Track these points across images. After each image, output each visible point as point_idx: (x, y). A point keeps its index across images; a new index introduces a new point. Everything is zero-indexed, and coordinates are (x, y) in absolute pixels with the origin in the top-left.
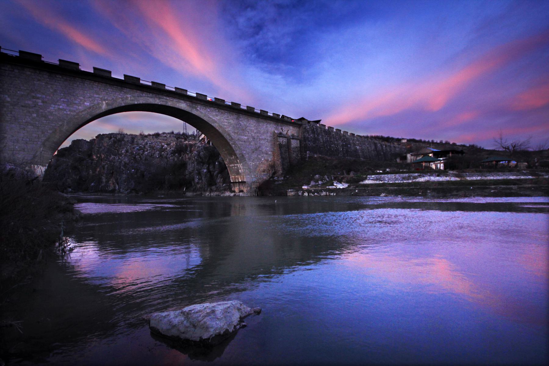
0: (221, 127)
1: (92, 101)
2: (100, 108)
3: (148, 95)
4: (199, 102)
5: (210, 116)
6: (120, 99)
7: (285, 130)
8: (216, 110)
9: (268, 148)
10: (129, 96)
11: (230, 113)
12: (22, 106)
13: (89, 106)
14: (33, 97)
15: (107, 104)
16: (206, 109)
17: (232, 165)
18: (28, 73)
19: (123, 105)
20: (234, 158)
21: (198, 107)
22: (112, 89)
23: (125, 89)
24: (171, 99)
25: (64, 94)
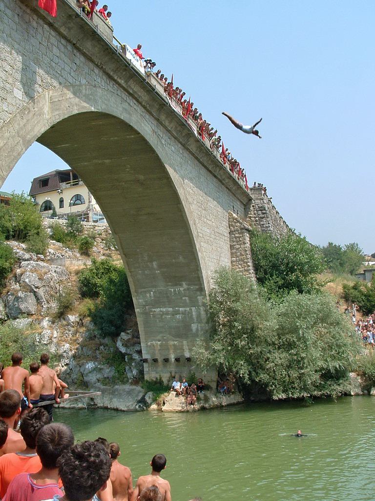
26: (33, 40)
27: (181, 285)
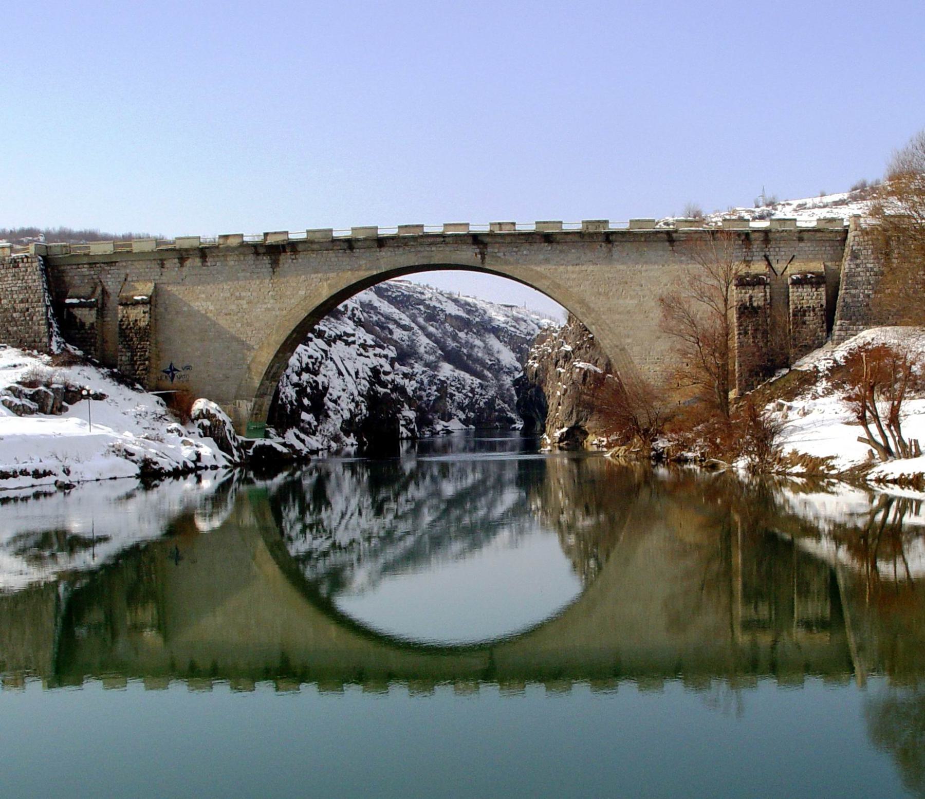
0: (559, 286)
2: (320, 294)
7: (777, 258)
10: (363, 262)
15: (330, 286)
16: (519, 251)
19: (354, 281)
21: (499, 252)
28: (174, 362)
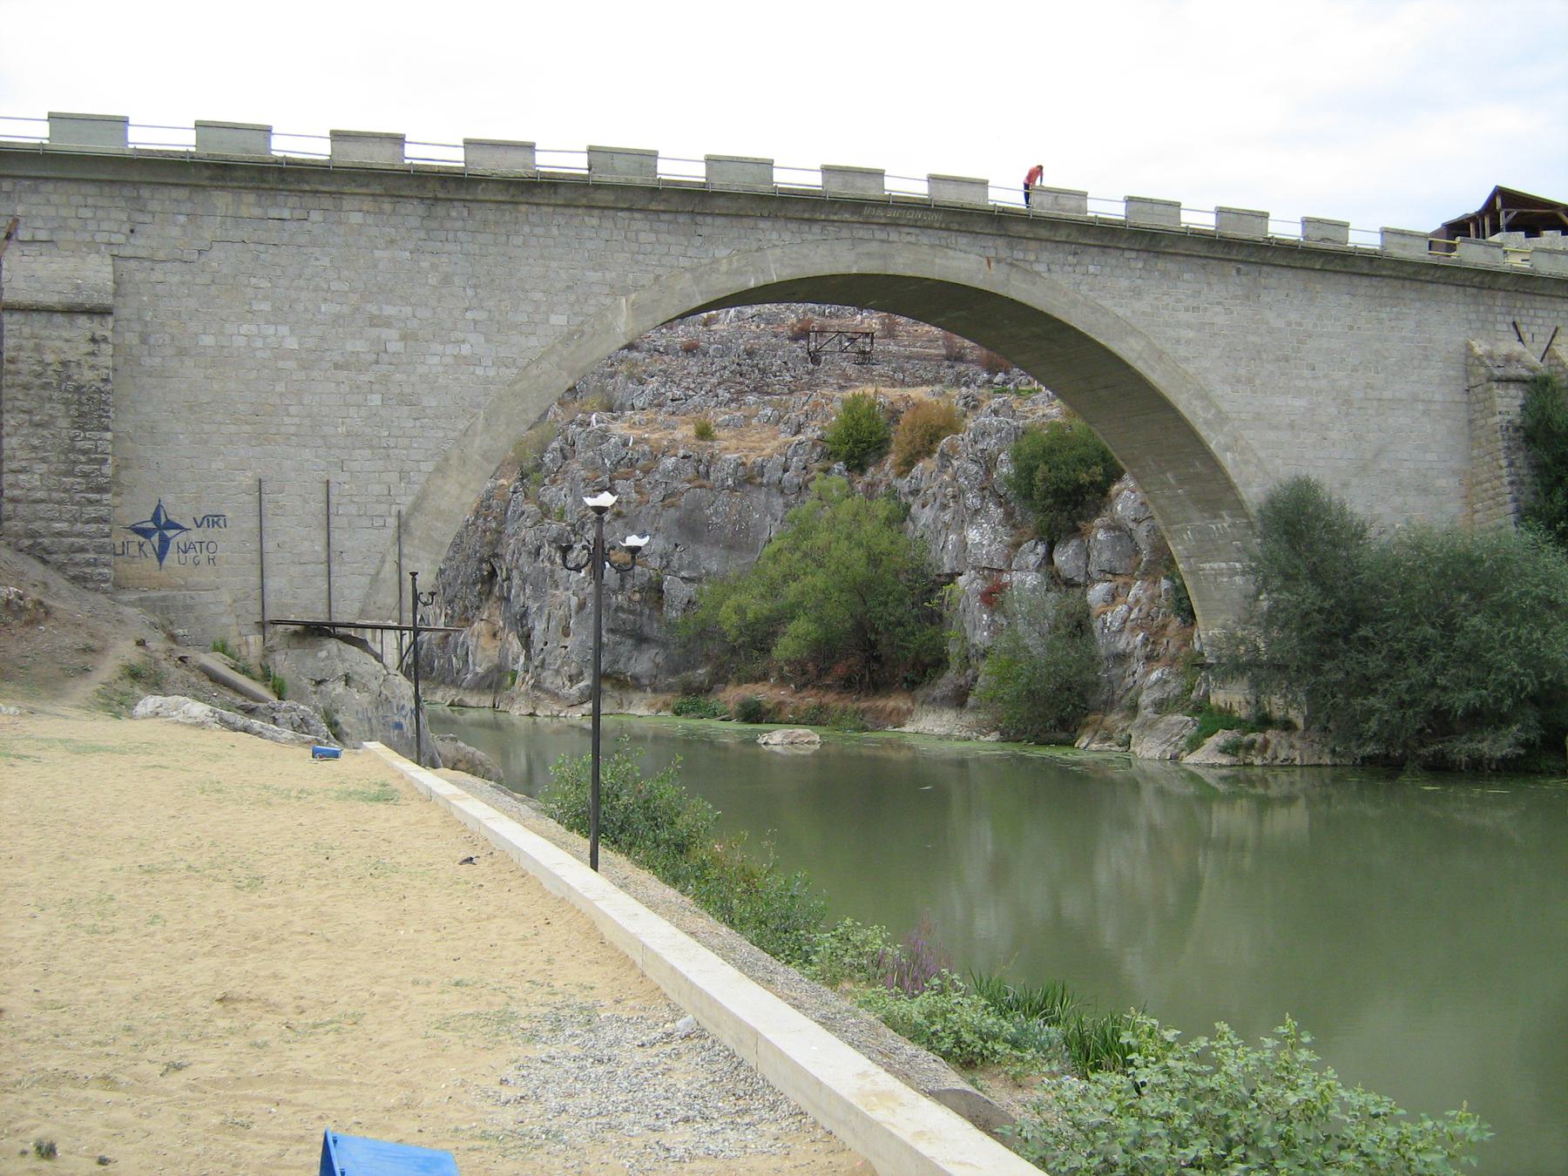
0: (1160, 355)
1: (578, 300)
3: (805, 236)
4: (1043, 233)
5: (1103, 303)
6: (688, 275)
8: (1133, 264)
9: (1430, 457)
10: (721, 253)
11: (1204, 266)
12: (337, 366)
13: (566, 330)
14: (374, 321)
15: (637, 309)
16: (1079, 263)
17: (1216, 566)
18: (356, 218)
20: (1233, 525)
21: (1037, 260)
22: (657, 232)
23: (709, 220)
24: (909, 238)
25: (475, 287)
26: (589, 245)
27: (1221, 517)
28: (169, 500)
